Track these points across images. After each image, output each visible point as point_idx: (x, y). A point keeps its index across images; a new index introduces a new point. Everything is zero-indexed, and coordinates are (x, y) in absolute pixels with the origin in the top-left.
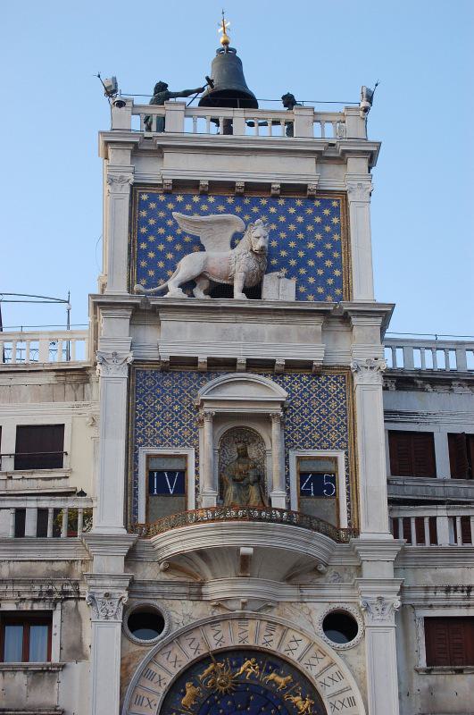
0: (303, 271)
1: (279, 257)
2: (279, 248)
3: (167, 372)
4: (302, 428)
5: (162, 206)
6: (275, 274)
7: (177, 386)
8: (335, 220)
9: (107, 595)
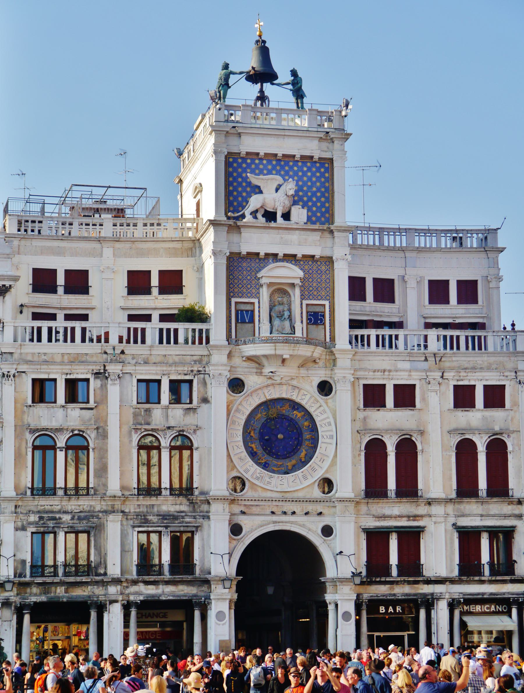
0: (310, 204)
3: (244, 258)
4: (308, 289)
9: (220, 374)
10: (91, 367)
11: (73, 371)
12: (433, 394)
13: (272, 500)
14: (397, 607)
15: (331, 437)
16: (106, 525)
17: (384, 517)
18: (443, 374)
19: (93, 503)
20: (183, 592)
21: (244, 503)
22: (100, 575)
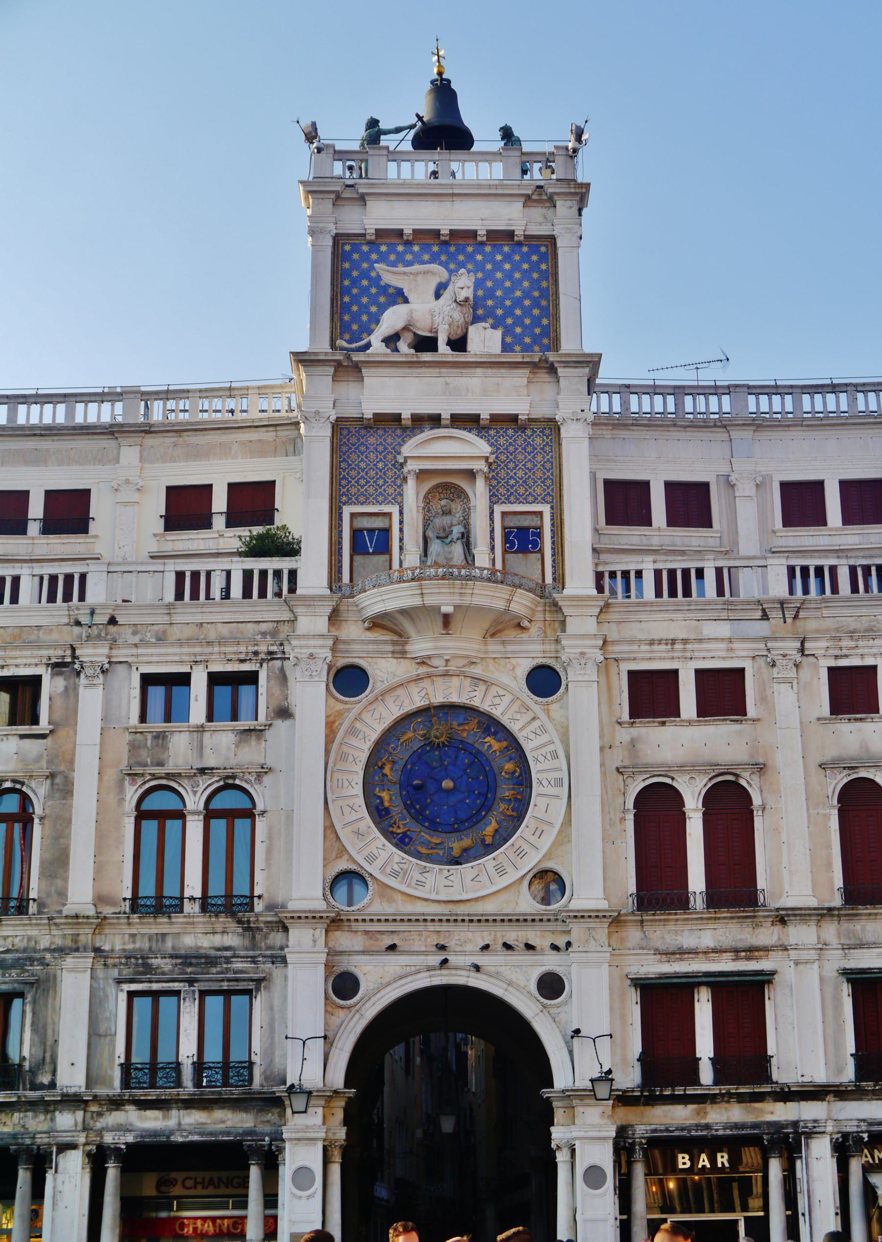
0: (509, 321)
1: (485, 307)
2: (485, 298)
3: (371, 428)
4: (507, 482)
5: (365, 257)
6: (480, 324)
7: (381, 443)
8: (544, 267)
9: (311, 655)
10: (45, 653)
11: (9, 662)
12: (785, 687)
13: (425, 920)
14: (719, 1155)
15: (559, 783)
16: (58, 980)
17: (681, 953)
18: (802, 643)
19: (33, 932)
20: (223, 1126)
21: (362, 927)
22: (42, 1087)
